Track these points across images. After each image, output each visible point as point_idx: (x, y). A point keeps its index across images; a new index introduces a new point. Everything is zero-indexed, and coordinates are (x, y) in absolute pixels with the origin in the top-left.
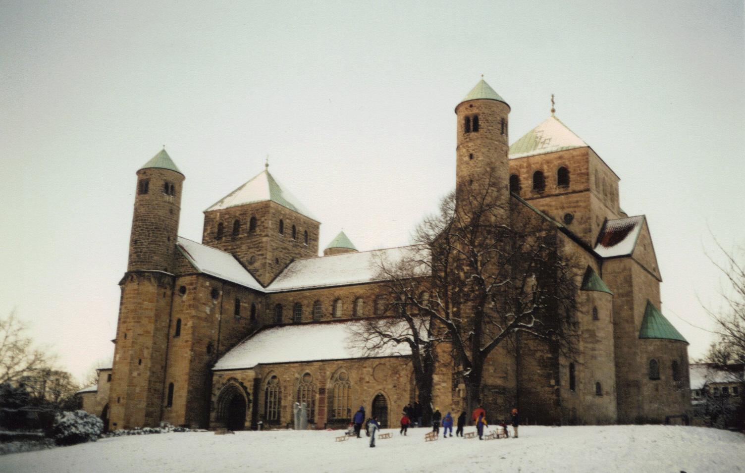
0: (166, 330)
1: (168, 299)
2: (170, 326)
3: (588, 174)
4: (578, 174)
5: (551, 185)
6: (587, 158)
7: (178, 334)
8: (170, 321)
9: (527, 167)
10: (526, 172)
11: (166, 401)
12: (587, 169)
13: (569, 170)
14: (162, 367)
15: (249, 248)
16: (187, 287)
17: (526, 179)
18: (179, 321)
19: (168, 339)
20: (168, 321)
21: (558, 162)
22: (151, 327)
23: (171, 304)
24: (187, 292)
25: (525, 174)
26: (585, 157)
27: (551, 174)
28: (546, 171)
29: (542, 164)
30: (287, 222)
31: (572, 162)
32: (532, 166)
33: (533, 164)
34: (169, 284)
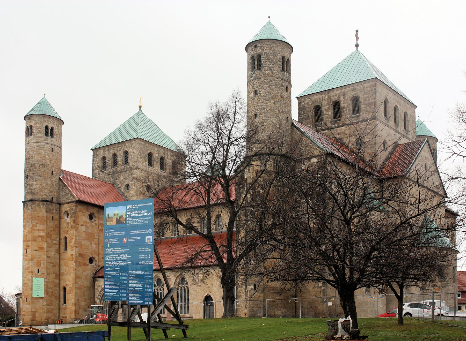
0: (57, 246)
1: (57, 222)
2: (60, 244)
3: (375, 104)
4: (367, 104)
5: (347, 114)
6: (375, 89)
7: (66, 249)
8: (60, 239)
9: (328, 99)
10: (327, 103)
11: (62, 300)
12: (375, 99)
13: (361, 100)
14: (56, 275)
15: (125, 179)
16: (69, 212)
17: (327, 110)
18: (66, 239)
19: (59, 254)
20: (58, 239)
21: (352, 93)
22: (45, 245)
23: (59, 227)
24: (69, 216)
25: (326, 105)
26: (373, 88)
27: (346, 104)
28: (342, 102)
29: (339, 96)
30: (156, 156)
31: (362, 93)
32: (332, 98)
33: (332, 96)
34: (56, 210)
